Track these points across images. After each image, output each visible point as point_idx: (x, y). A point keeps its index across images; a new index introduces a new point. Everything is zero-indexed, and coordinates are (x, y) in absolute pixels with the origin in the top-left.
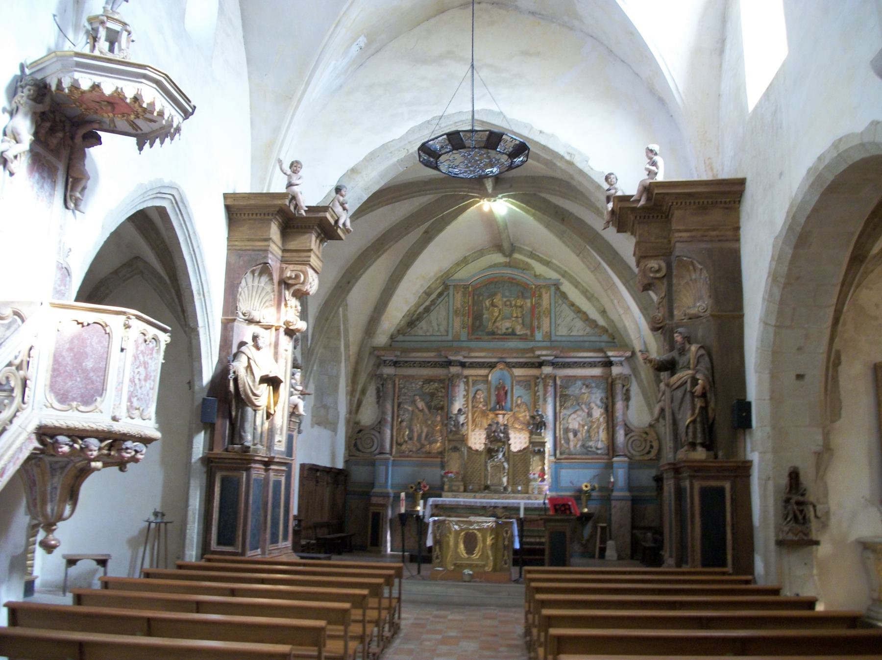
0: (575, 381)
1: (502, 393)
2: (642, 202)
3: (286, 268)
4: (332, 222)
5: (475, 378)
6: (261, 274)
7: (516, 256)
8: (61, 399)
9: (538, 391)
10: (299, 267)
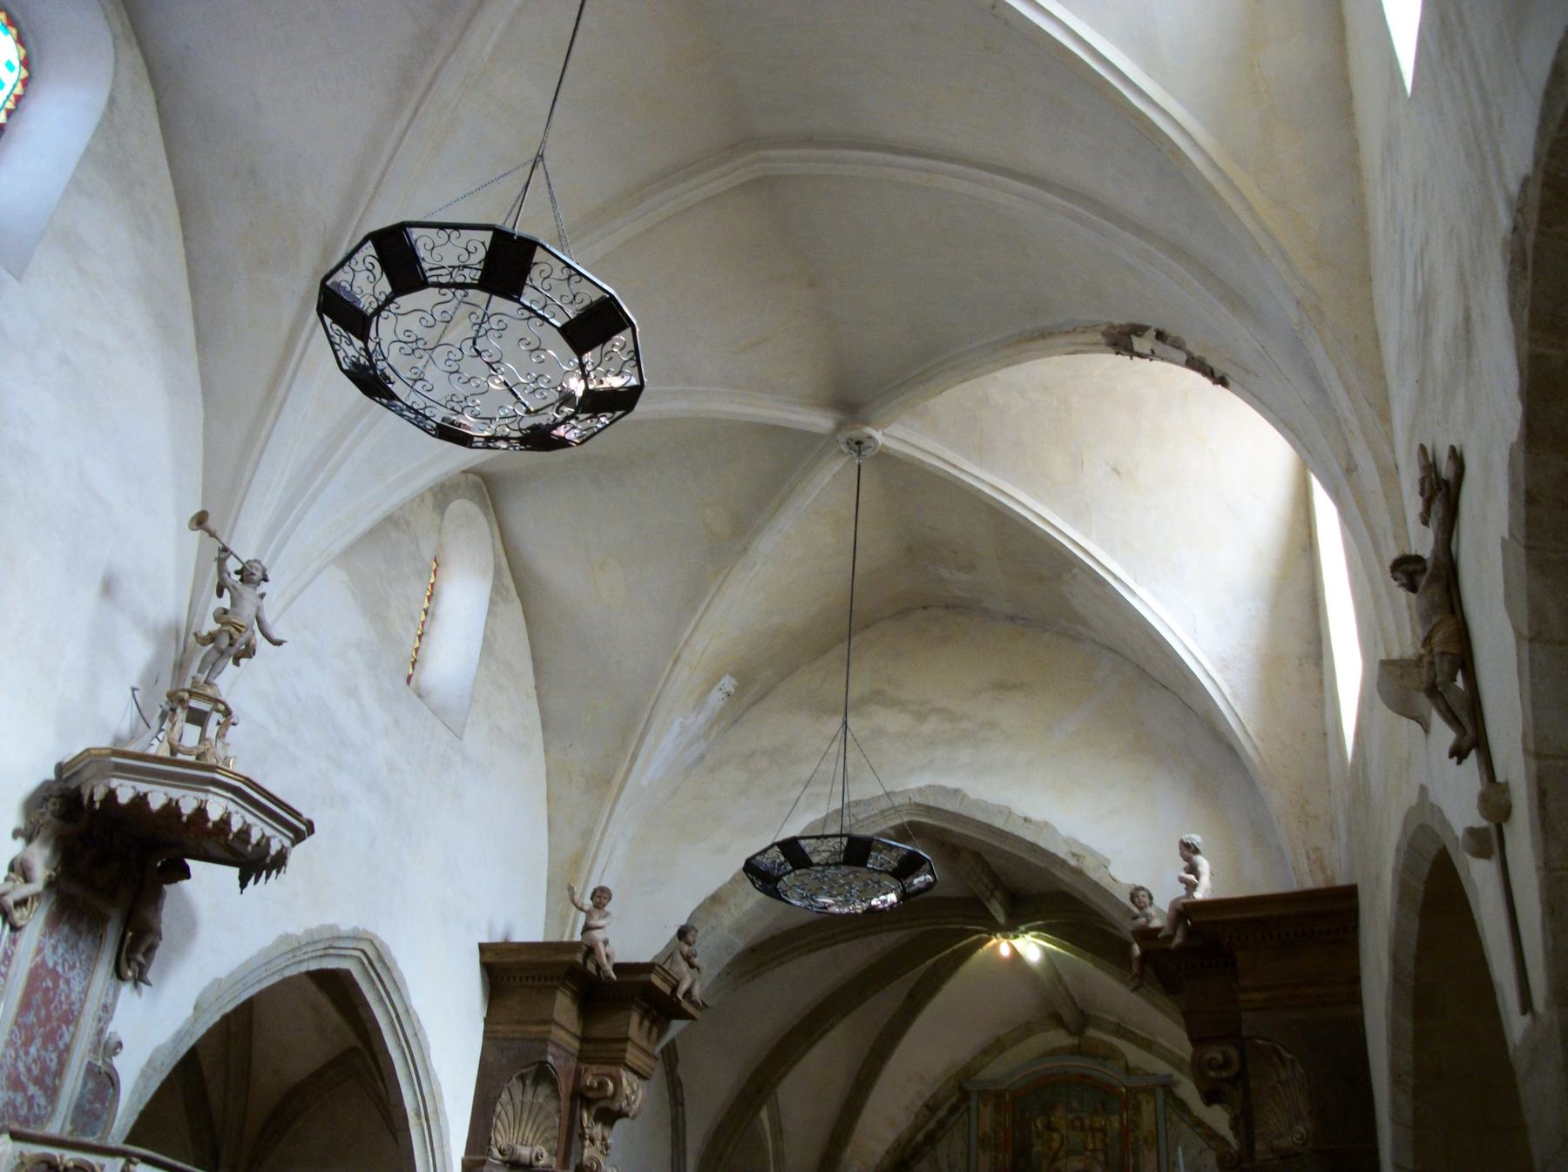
2: (1178, 940)
3: (586, 1070)
4: (667, 989)
6: (536, 1082)
7: (1092, 1032)
10: (606, 1069)
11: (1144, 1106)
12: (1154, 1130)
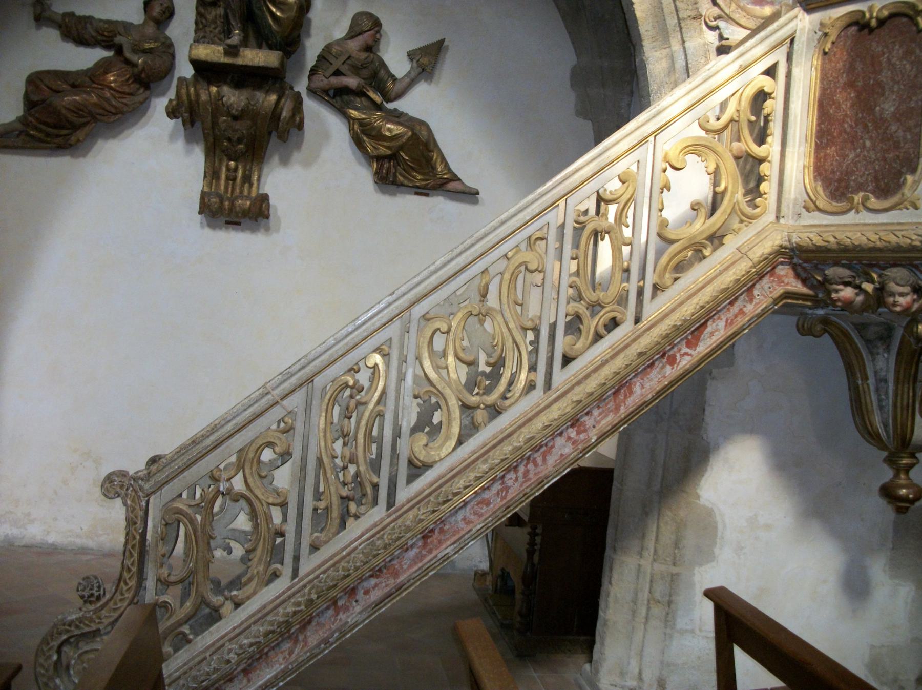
8: (837, 190)
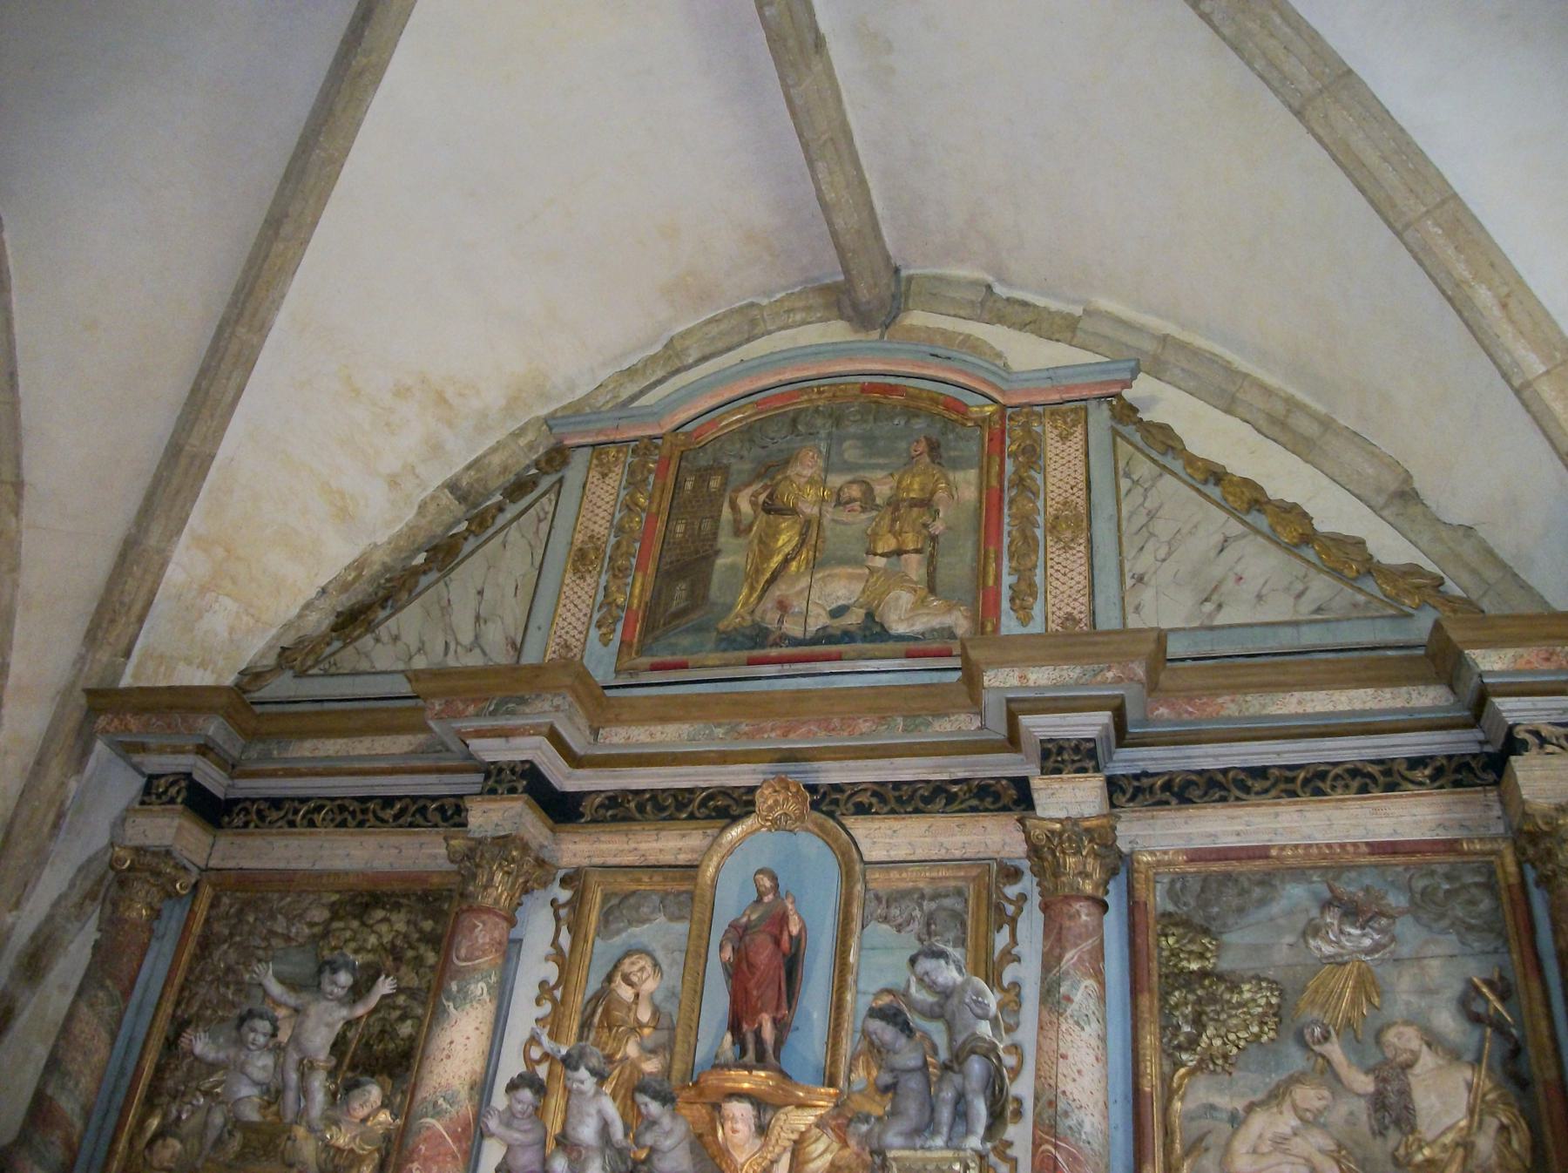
0: (1266, 880)
1: (764, 954)
5: (624, 884)
7: (917, 318)
9: (1010, 956)
11: (1053, 447)
12: (1082, 502)
